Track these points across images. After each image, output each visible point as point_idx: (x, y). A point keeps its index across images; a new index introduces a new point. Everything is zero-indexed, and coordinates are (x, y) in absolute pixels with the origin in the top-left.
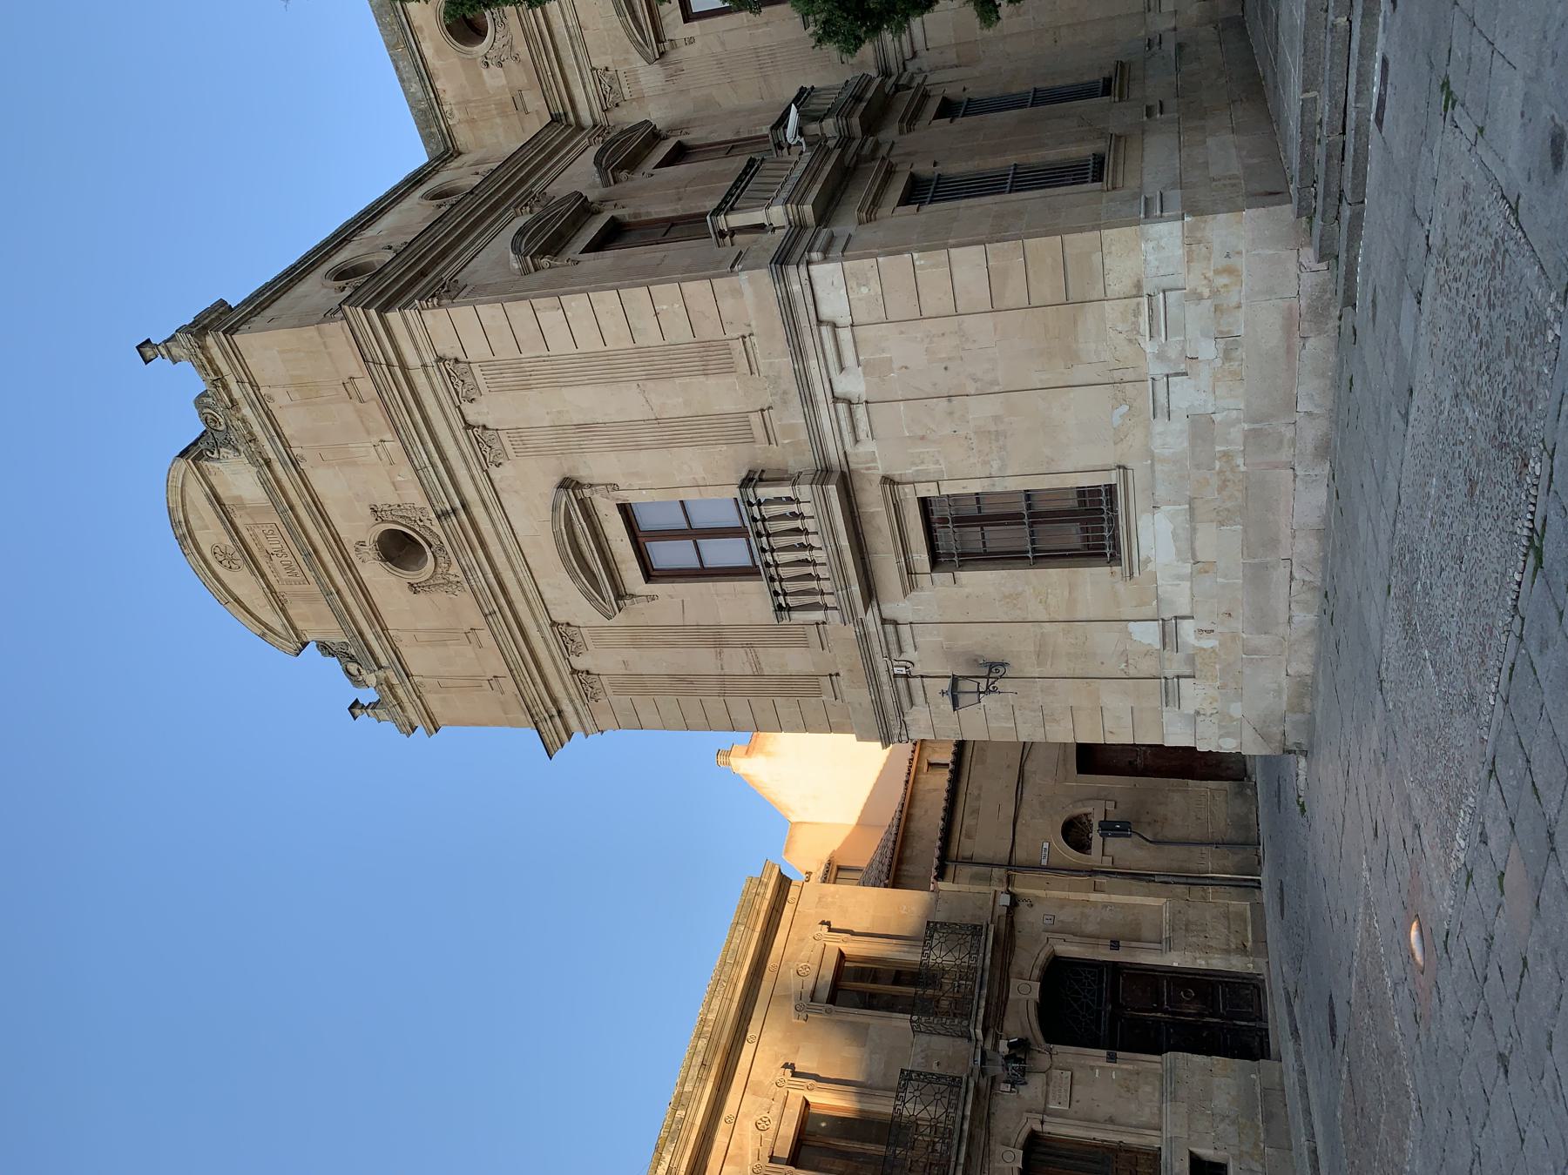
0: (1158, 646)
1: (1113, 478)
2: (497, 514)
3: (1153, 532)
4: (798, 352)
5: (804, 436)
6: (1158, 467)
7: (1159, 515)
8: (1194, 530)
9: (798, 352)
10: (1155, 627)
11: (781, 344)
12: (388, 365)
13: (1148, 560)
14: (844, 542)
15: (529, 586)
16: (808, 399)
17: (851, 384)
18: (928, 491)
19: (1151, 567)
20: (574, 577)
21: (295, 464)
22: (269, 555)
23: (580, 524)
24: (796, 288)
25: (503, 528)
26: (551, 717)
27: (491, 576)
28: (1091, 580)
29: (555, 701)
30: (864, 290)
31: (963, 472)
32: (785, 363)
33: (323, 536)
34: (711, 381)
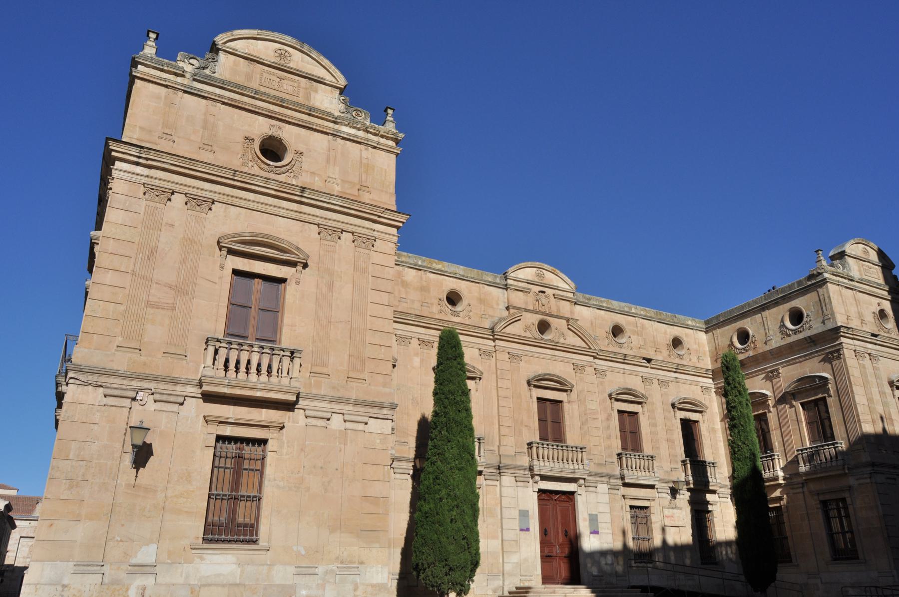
0: (134, 561)
1: (262, 542)
2: (293, 215)
3: (224, 562)
4: (358, 403)
5: (314, 391)
6: (266, 567)
7: (234, 566)
8: (223, 586)
9: (358, 403)
10: (151, 560)
11: (362, 397)
12: (379, 217)
13: (202, 559)
14: (259, 394)
15: (243, 203)
16: (335, 400)
17: (337, 422)
18: (270, 445)
19: (197, 560)
20: (252, 234)
21: (333, 135)
22: (281, 79)
23: (285, 257)
24: (385, 412)
25: (283, 212)
26: (139, 157)
27: (257, 188)
28: (198, 527)
29: (150, 167)
30: (378, 441)
31: (278, 466)
32: (353, 395)
33: (293, 118)
34: (346, 357)
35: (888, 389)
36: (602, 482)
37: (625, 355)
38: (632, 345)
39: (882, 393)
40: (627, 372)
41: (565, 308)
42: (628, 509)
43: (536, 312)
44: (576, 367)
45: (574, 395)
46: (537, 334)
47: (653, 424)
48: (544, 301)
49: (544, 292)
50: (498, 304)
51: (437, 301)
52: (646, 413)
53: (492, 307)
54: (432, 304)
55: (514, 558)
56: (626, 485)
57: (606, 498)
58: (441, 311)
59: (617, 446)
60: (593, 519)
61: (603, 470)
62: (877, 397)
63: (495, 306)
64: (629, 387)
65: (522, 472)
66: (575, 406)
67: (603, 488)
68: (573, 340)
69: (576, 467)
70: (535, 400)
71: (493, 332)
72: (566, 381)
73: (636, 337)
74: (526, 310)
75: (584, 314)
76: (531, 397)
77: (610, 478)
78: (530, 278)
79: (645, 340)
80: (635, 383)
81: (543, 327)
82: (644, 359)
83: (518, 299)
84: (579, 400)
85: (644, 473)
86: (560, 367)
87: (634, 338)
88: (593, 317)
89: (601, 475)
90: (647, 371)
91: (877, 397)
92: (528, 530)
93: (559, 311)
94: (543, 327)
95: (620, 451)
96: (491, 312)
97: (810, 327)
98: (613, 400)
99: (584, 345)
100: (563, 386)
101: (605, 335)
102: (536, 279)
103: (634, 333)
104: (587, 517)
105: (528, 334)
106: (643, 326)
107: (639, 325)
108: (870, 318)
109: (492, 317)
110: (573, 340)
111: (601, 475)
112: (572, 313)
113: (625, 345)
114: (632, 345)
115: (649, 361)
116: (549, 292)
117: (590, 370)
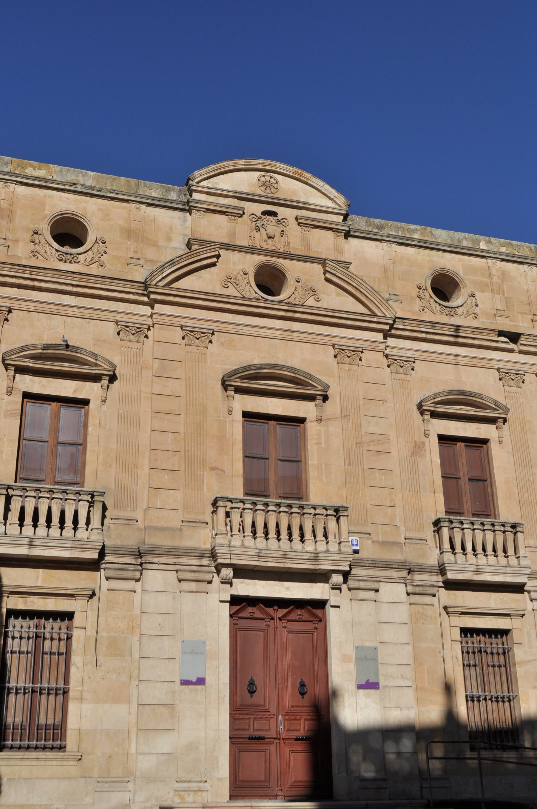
36: (392, 580)
37: (458, 328)
38: (477, 310)
40: (462, 360)
41: (324, 243)
42: (457, 635)
43: (252, 250)
44: (340, 351)
45: (331, 407)
46: (253, 291)
49: (274, 214)
50: (169, 239)
51: (28, 236)
52: (507, 440)
53: (155, 245)
54: (17, 241)
55: (164, 744)
56: (452, 585)
57: (402, 613)
58: (35, 254)
59: (435, 505)
60: (367, 657)
61: (396, 556)
63: (161, 243)
64: (468, 388)
65: (194, 561)
66: (335, 428)
67: (393, 591)
68: (334, 300)
69: (321, 546)
70: (239, 417)
71: (146, 288)
72: (311, 377)
73: (487, 295)
74: (227, 247)
75: (365, 255)
76: (230, 412)
77: (410, 572)
78: (244, 188)
79: (507, 300)
80: (482, 382)
81: (270, 280)
82: (501, 333)
83: (216, 228)
85: (492, 559)
86: (303, 352)
87: (482, 297)
88: (390, 263)
89: (389, 566)
90: (513, 359)
92: (201, 681)
93: (308, 246)
94: (270, 280)
95: (442, 514)
96: (151, 253)
98: (427, 417)
99: (362, 309)
100: (302, 387)
101: (415, 292)
103: (483, 287)
104: (350, 651)
105: (231, 291)
106: (504, 275)
107: (494, 272)
109: (152, 261)
110: (334, 300)
111: (389, 566)
112: (339, 251)
114: (477, 310)
115: (514, 337)
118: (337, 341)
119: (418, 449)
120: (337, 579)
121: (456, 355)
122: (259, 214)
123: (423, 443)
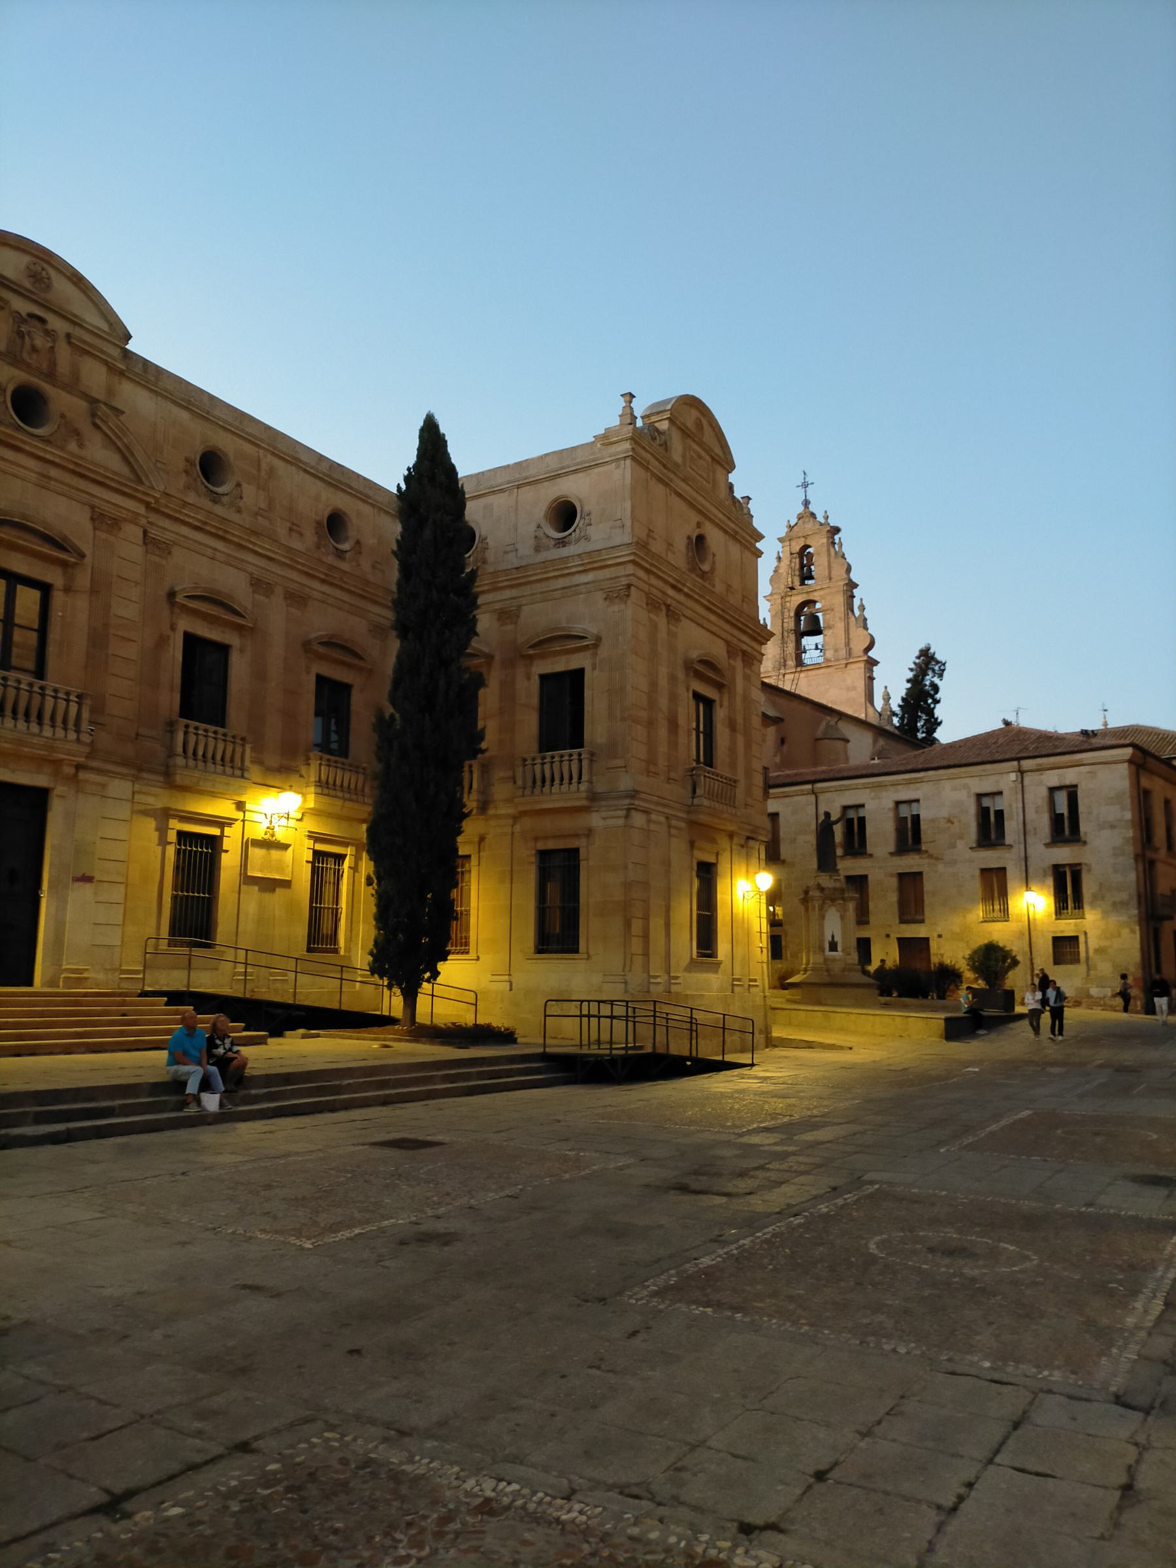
35: (681, 675)
38: (241, 504)
39: (673, 678)
40: (219, 556)
45: (83, 580)
47: (260, 674)
48: (40, 341)
49: (42, 321)
62: (663, 682)
68: (98, 454)
80: (233, 582)
84: (94, 591)
91: (663, 682)
97: (587, 539)
98: (177, 610)
99: (125, 470)
102: (27, 284)
108: (681, 544)
110: (98, 454)
112: (110, 392)
113: (225, 499)
116: (55, 323)
117: (133, 532)
118: (96, 502)
119: (162, 642)
120: (69, 770)
121: (215, 549)
122: (24, 314)
123: (168, 637)
